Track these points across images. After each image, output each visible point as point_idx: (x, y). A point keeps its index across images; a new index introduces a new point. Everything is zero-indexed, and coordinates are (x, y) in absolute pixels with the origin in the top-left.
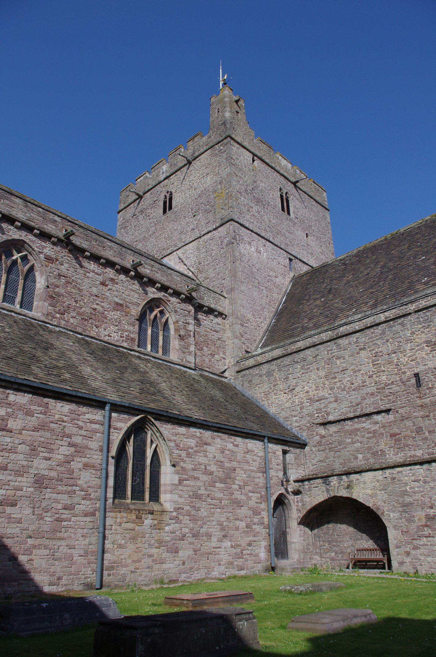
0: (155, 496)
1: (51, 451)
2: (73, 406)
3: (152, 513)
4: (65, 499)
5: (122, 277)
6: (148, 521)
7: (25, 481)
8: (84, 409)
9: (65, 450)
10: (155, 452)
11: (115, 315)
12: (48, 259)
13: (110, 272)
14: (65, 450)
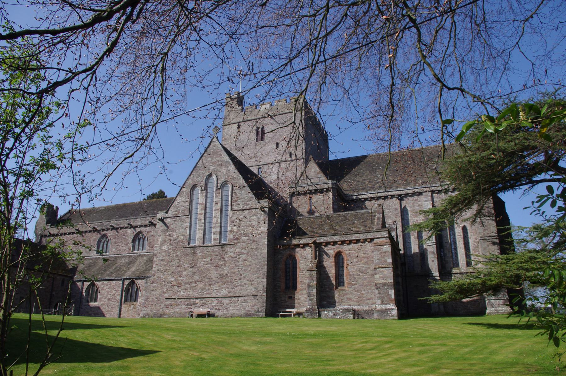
0: (136, 300)
1: (111, 293)
2: (116, 281)
3: (133, 304)
7: (106, 300)
8: (118, 281)
9: (114, 292)
12: (149, 232)
14: (114, 292)
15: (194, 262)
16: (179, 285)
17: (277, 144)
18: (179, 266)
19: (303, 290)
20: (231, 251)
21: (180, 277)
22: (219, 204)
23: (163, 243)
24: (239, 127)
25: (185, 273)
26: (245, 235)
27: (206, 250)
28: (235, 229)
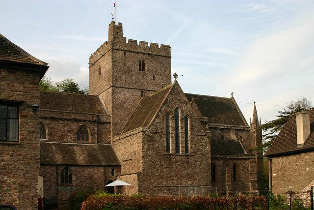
0: (71, 182)
4: (49, 184)
5: (70, 122)
6: (69, 187)
9: (49, 175)
10: (71, 173)
11: (69, 134)
12: (48, 124)
13: (66, 122)
14: (49, 175)
15: (171, 163)
16: (162, 178)
17: (154, 77)
18: (161, 166)
19: (219, 182)
20: (192, 160)
21: (162, 173)
22: (184, 129)
23: (148, 149)
24: (125, 53)
25: (165, 170)
26: (200, 150)
27: (177, 157)
28: (194, 146)
